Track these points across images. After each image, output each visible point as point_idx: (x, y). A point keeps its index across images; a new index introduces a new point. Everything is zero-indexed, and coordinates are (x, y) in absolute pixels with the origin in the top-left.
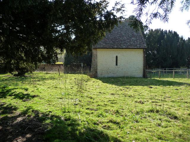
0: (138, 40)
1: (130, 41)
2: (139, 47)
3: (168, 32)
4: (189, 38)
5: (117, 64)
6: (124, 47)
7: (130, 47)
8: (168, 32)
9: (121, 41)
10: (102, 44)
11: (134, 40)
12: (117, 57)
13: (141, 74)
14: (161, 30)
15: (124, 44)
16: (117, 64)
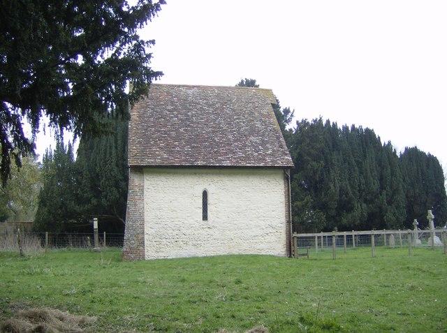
0: (267, 142)
1: (245, 146)
2: (270, 164)
3: (350, 129)
4: (406, 149)
5: (205, 217)
6: (227, 163)
7: (243, 164)
8: (350, 129)
9: (218, 144)
10: (159, 155)
11: (256, 143)
12: (205, 194)
13: (279, 249)
14: (324, 123)
15: (226, 154)
16: (205, 217)
